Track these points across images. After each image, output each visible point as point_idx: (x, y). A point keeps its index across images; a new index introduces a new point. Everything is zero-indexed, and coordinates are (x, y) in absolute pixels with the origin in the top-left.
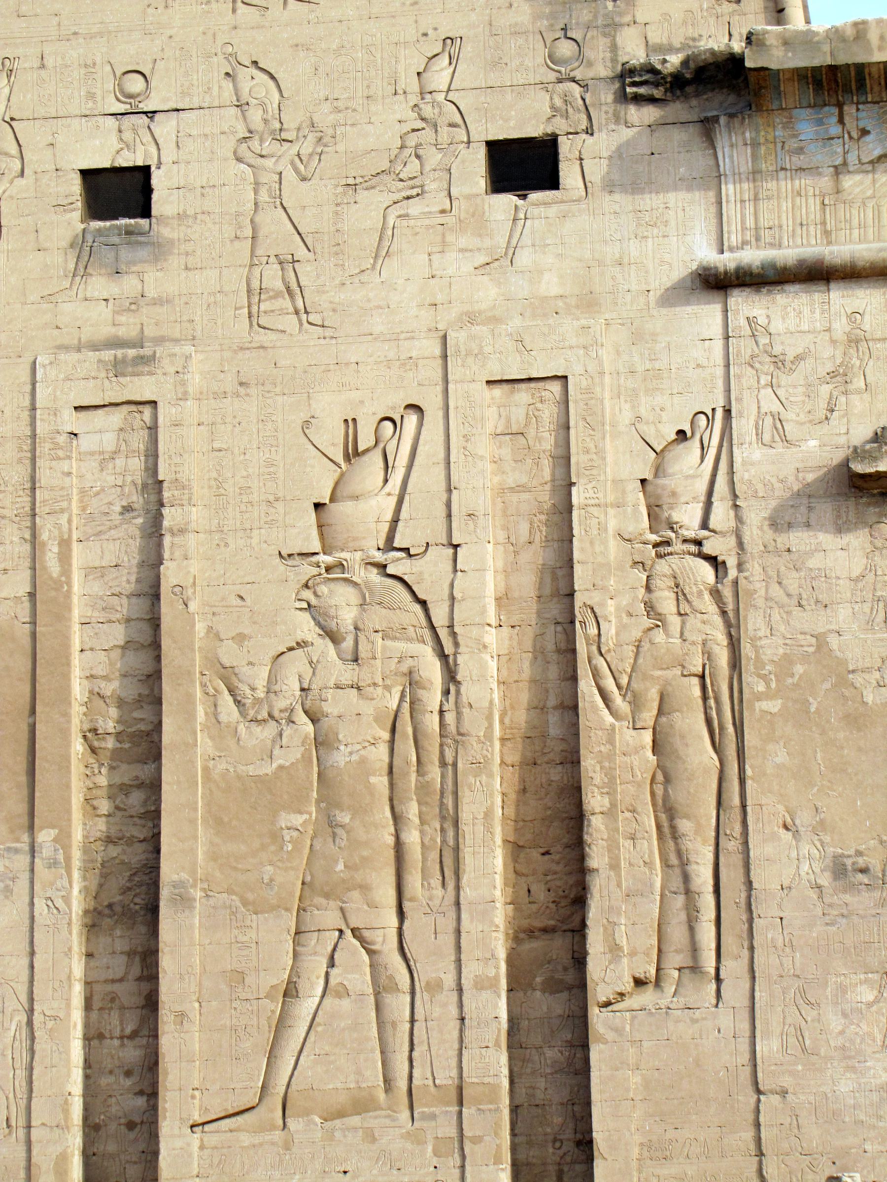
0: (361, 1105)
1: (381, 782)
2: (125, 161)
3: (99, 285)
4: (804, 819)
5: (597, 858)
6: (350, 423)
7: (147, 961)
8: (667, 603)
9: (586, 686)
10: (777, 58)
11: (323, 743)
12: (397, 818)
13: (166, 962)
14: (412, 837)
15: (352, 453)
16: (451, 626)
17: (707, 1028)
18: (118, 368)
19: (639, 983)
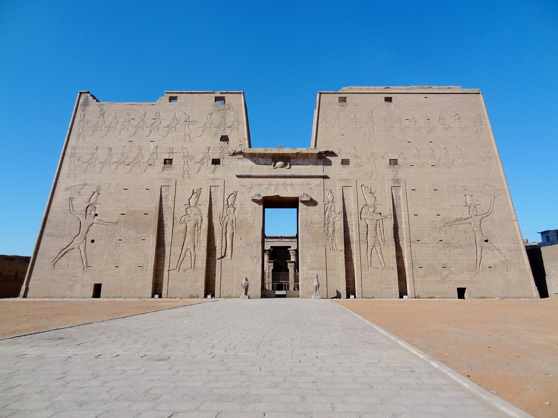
3: (165, 172)
6: (193, 190)
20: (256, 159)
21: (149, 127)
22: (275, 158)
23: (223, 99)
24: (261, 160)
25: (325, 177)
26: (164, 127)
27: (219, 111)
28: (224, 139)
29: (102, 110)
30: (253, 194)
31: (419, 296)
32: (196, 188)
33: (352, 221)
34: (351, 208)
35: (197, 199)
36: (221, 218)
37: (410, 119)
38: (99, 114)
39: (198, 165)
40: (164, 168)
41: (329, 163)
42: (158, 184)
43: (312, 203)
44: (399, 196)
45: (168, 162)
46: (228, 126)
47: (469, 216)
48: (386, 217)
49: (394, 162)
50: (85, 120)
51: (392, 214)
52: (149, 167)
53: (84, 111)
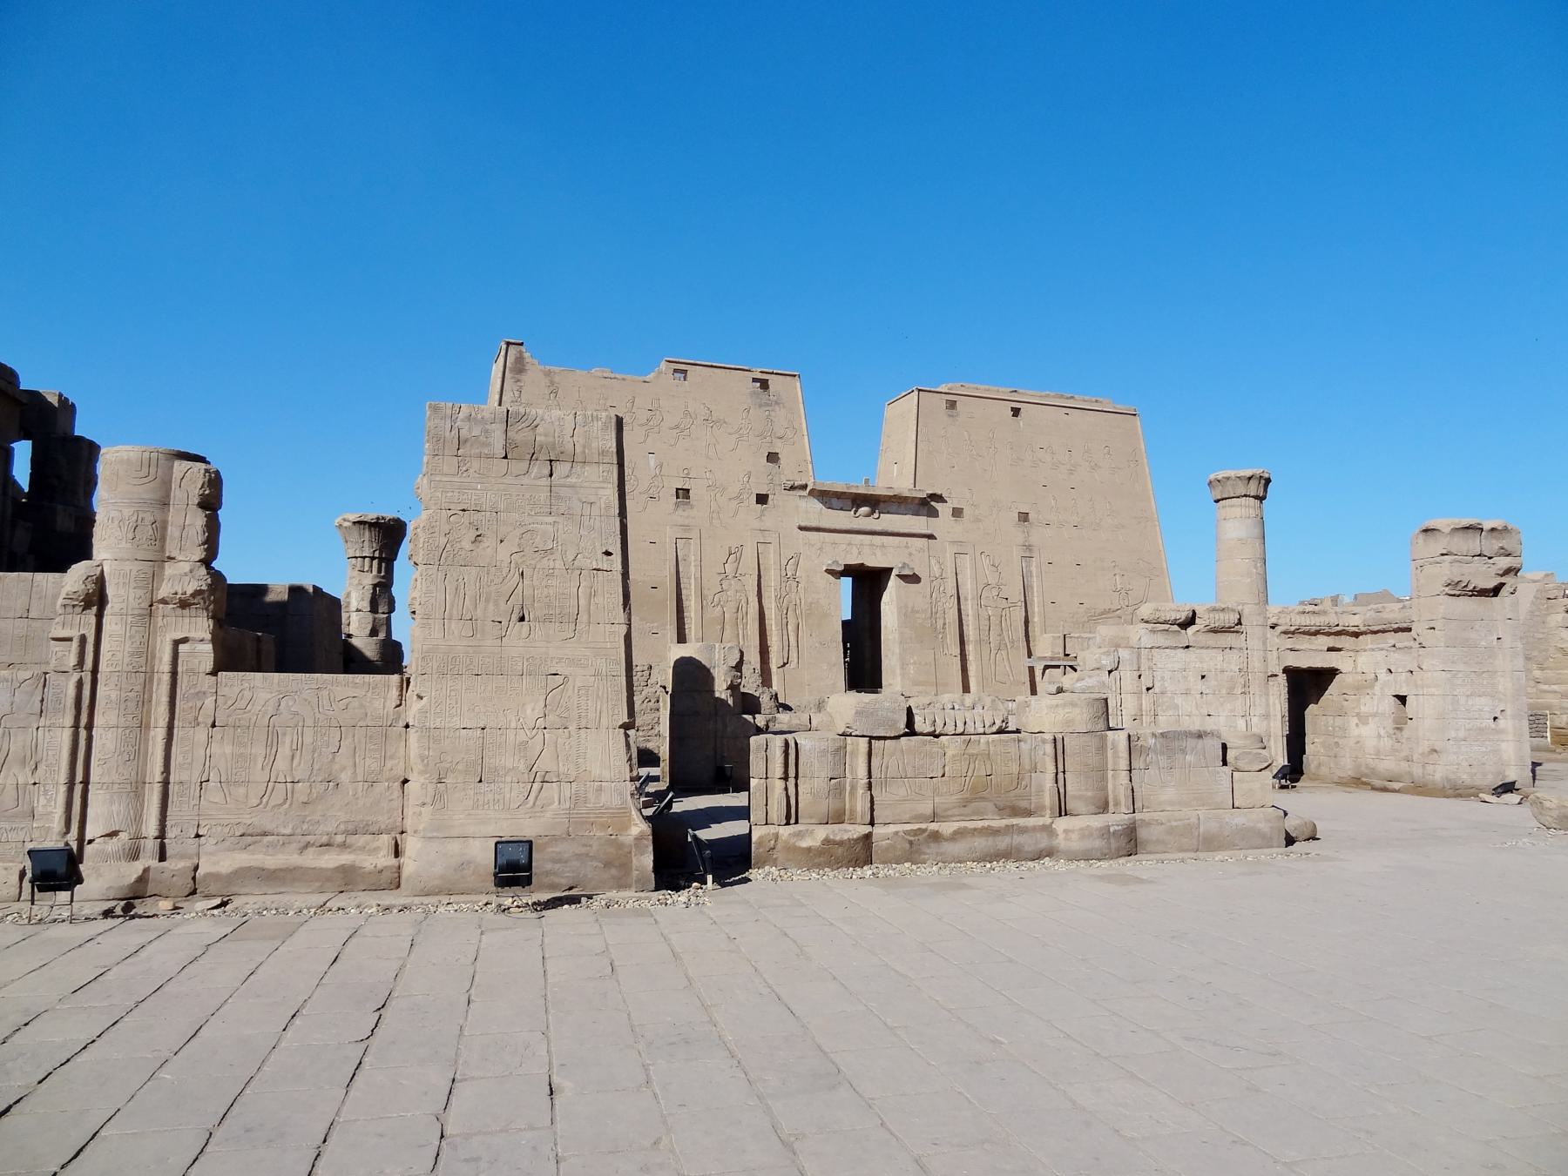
3: (680, 512)
22: (857, 501)
23: (764, 385)
24: (834, 501)
25: (931, 537)
28: (772, 457)
29: (552, 383)
30: (827, 562)
32: (734, 545)
33: (969, 608)
34: (968, 589)
36: (779, 599)
38: (547, 392)
41: (934, 513)
42: (670, 534)
43: (913, 579)
45: (683, 494)
48: (1014, 605)
49: (1024, 517)
52: (651, 502)
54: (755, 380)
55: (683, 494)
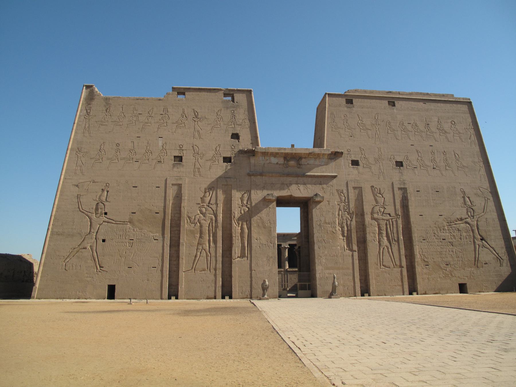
0: (204, 270)
1: (207, 231)
2: (179, 155)
3: (175, 169)
4: (258, 238)
5: (234, 242)
7: (178, 251)
8: (243, 212)
9: (233, 221)
10: (259, 150)
11: (201, 226)
12: (209, 236)
13: (181, 252)
14: (211, 238)
15: (205, 192)
16: (217, 213)
17: (245, 262)
18: (177, 179)
19: (238, 257)
20: (268, 158)
21: (158, 122)
26: (173, 123)
27: (227, 108)
28: (236, 136)
31: (426, 292)
35: (209, 198)
37: (412, 122)
38: (104, 109)
39: (209, 163)
40: (174, 166)
44: (405, 197)
45: (179, 159)
46: (238, 123)
47: (467, 216)
49: (400, 164)
50: (91, 114)
51: (400, 214)
53: (89, 104)
54: (226, 95)
55: (179, 159)
